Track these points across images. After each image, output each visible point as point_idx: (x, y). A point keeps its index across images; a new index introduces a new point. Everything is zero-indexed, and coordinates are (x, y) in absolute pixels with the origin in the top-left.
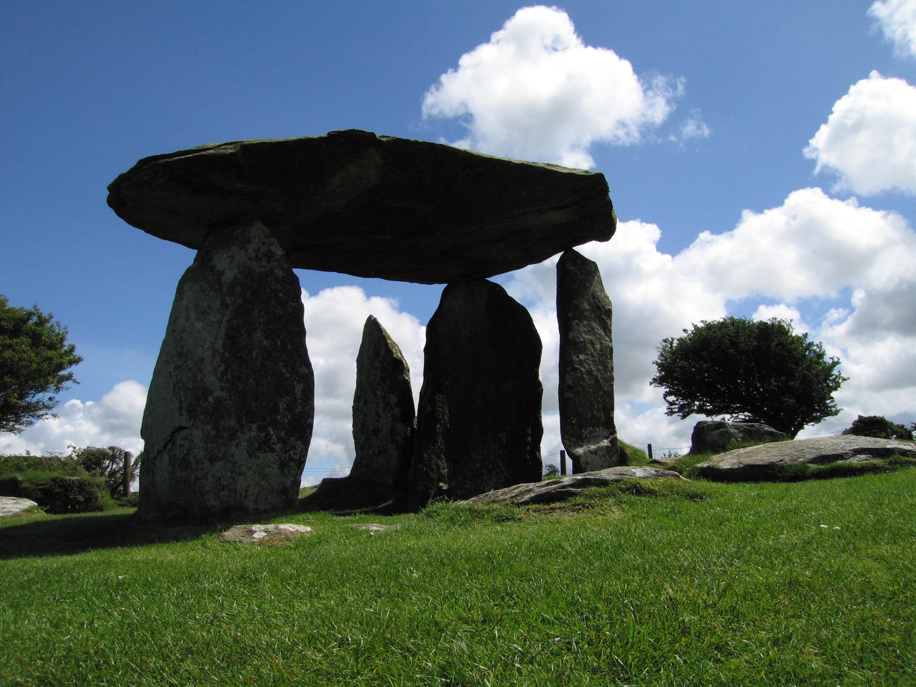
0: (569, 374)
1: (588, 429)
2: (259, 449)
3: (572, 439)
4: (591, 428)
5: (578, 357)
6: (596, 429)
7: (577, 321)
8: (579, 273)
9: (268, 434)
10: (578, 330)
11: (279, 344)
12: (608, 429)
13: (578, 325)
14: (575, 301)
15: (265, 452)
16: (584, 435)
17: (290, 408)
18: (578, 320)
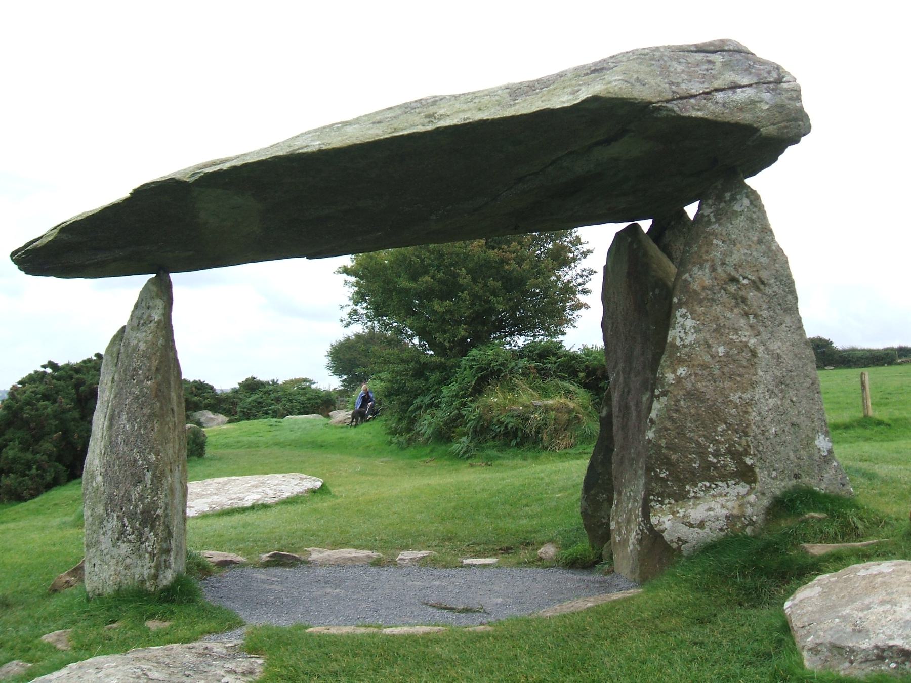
0: (658, 400)
1: (700, 485)
2: (118, 539)
3: (666, 501)
4: (708, 484)
5: (674, 372)
6: (720, 483)
7: (683, 310)
8: (713, 220)
9: (124, 525)
10: (682, 326)
11: (136, 428)
12: (749, 483)
13: (684, 316)
14: (687, 275)
15: (124, 542)
16: (692, 494)
17: (142, 498)
18: (688, 308)
